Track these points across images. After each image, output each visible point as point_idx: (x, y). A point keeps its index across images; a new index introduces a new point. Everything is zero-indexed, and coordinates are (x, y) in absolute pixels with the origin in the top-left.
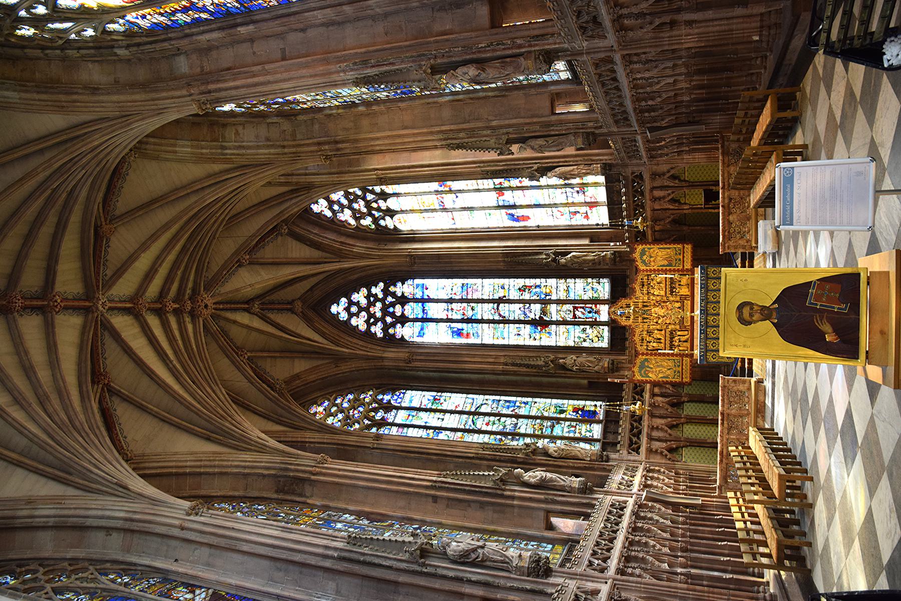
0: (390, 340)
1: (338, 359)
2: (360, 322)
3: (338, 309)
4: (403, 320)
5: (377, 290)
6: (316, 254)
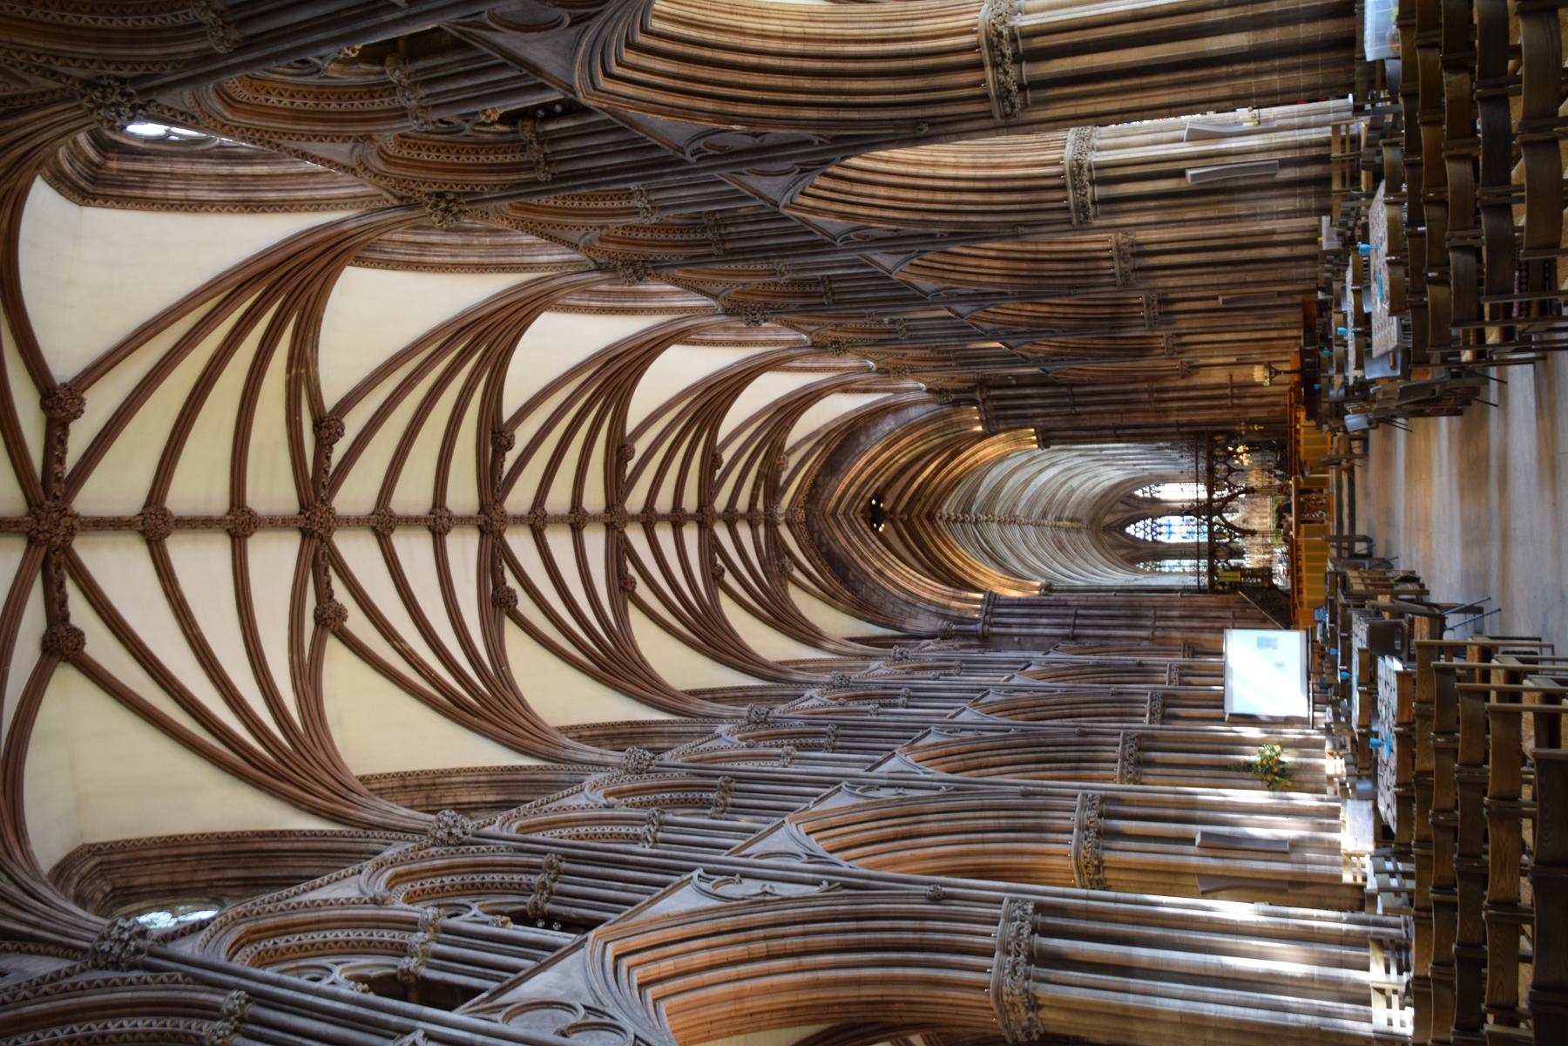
0: (1155, 541)
1: (1138, 549)
2: (1140, 535)
3: (1130, 530)
4: (1160, 534)
5: (1149, 521)
6: (1126, 507)
